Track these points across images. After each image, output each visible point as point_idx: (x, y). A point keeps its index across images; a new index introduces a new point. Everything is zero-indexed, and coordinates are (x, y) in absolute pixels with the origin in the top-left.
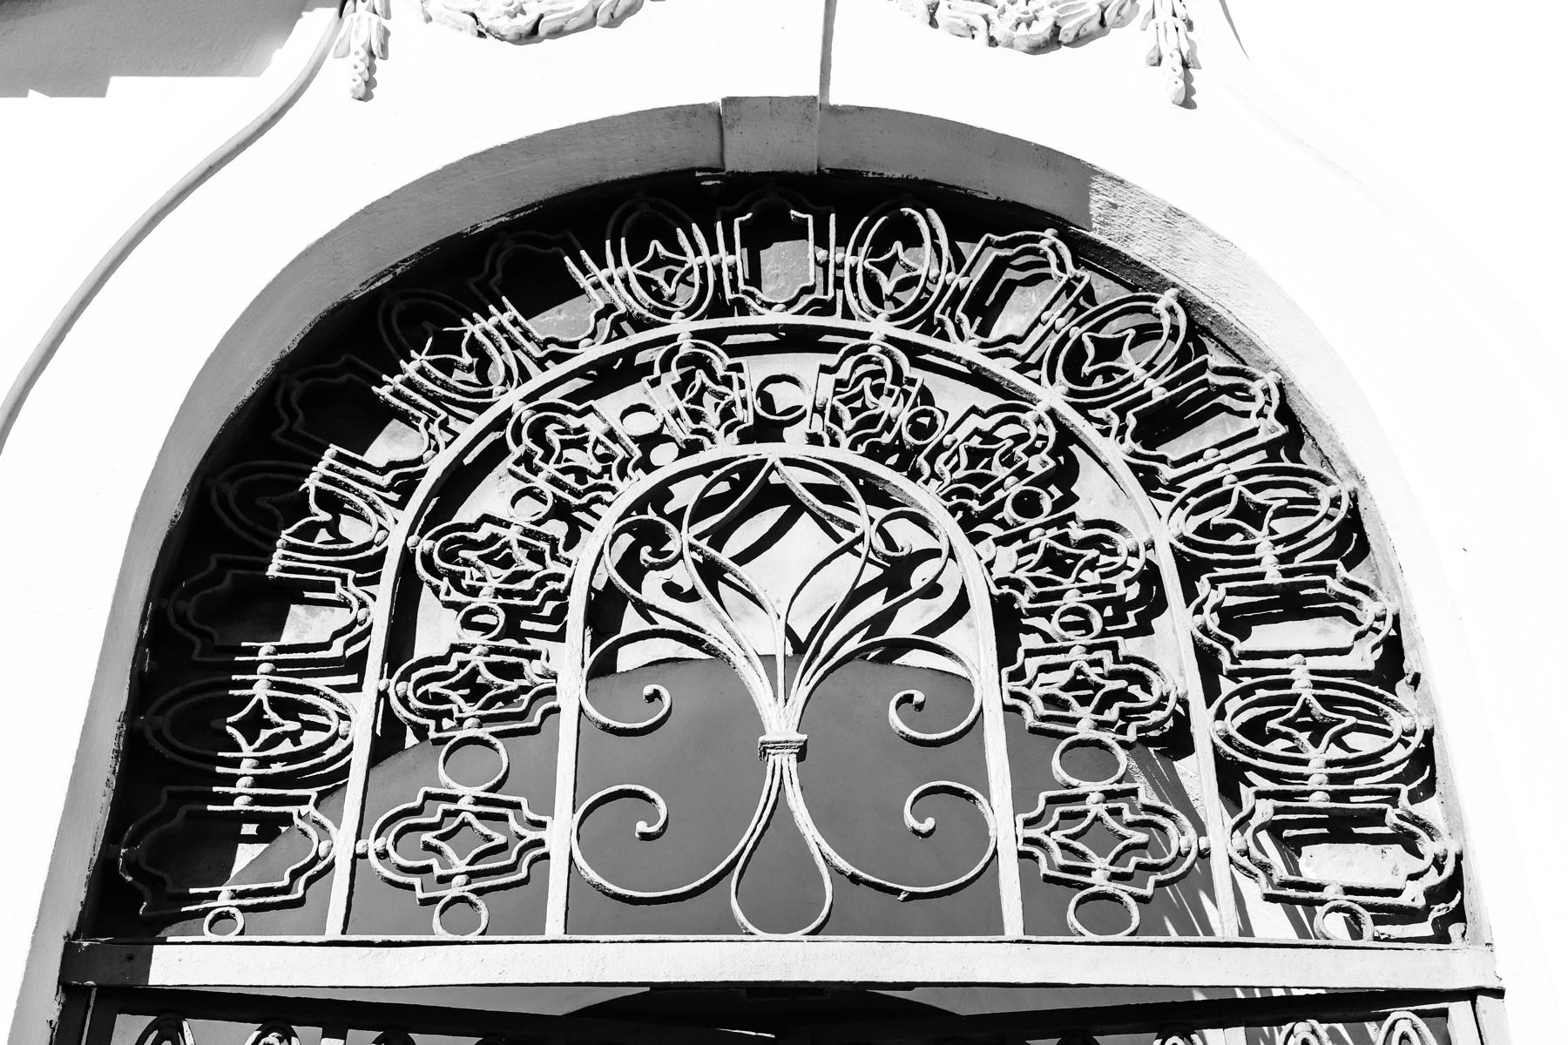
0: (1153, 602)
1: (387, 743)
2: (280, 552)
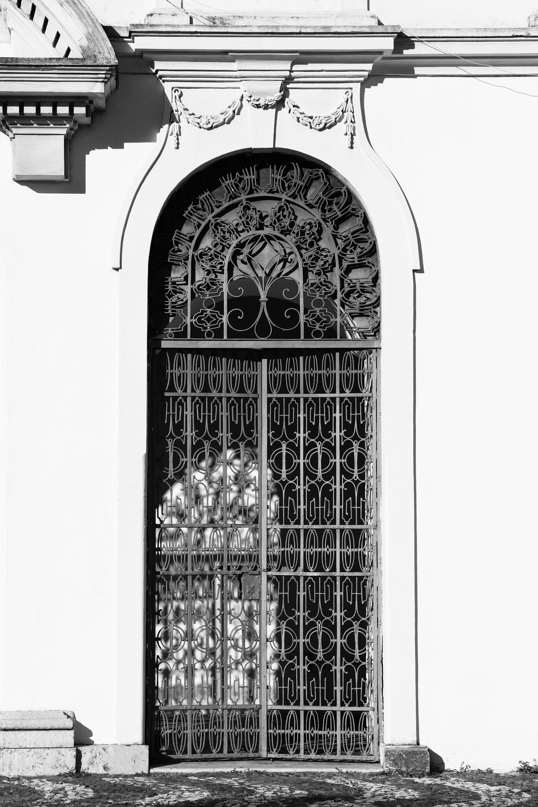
0: (333, 264)
2: (170, 256)
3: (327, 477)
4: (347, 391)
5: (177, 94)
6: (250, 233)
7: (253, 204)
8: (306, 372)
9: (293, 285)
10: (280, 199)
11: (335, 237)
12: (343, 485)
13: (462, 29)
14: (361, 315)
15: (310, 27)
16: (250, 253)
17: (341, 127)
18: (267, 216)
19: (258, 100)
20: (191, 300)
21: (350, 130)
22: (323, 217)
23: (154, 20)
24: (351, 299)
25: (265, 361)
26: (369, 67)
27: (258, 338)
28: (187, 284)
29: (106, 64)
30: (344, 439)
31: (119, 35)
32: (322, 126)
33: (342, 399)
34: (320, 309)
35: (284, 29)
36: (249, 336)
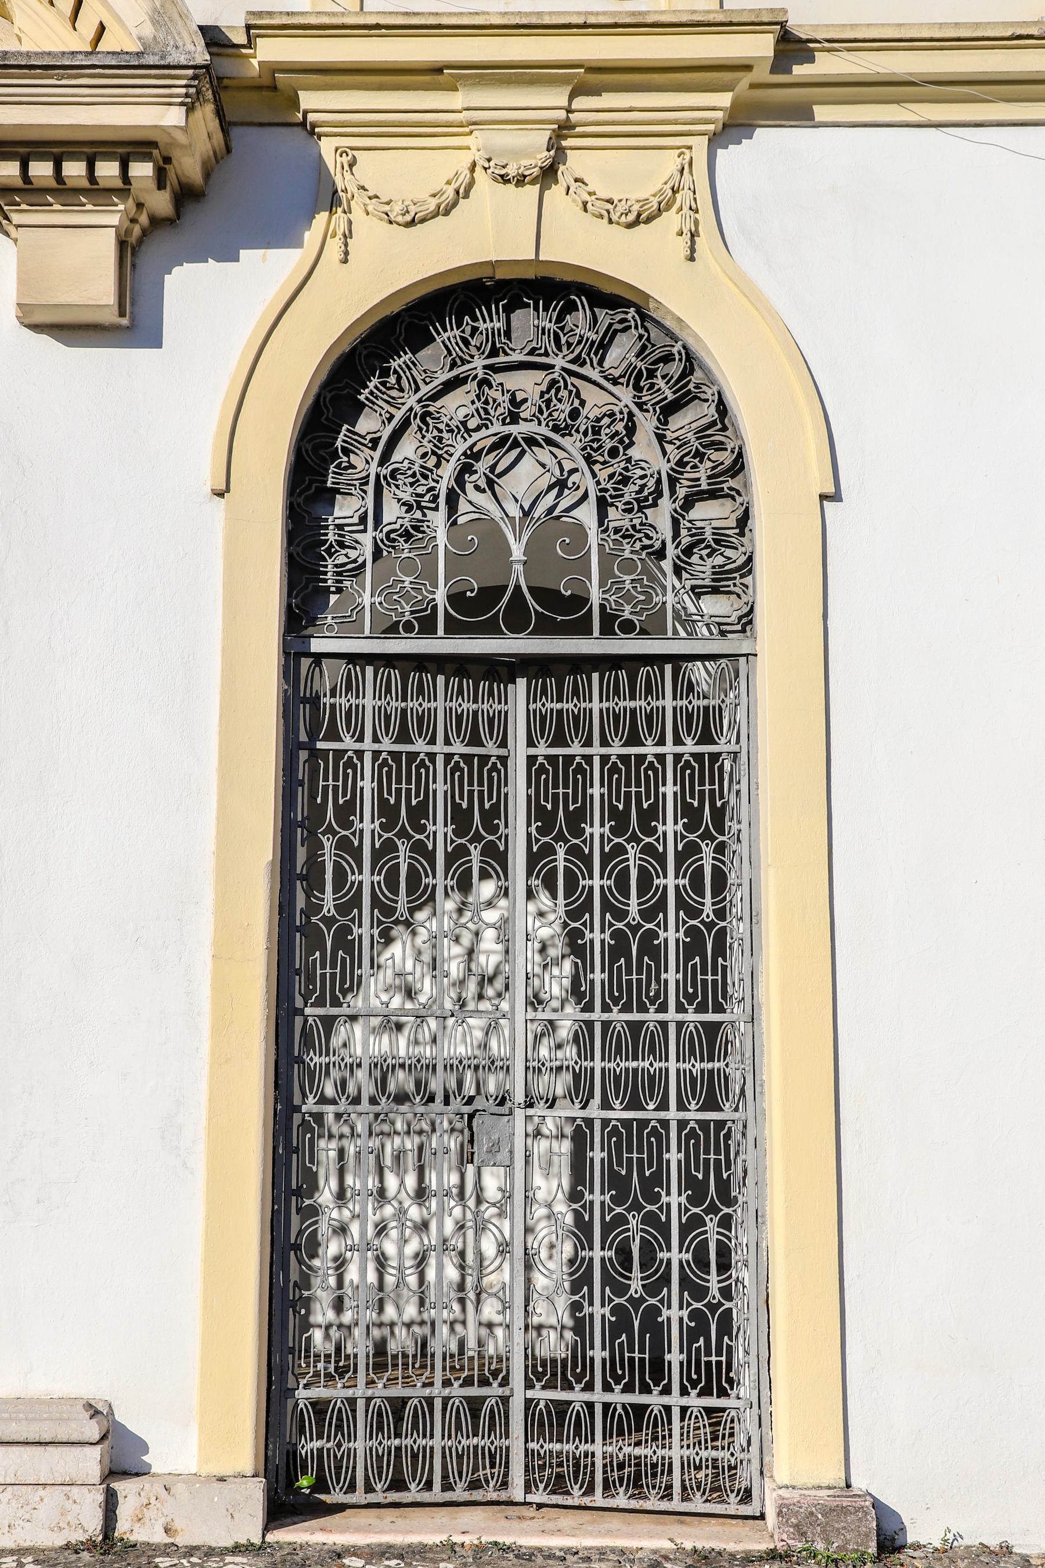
0: (658, 493)
1: (377, 554)
2: (331, 475)
3: (648, 914)
4: (689, 741)
5: (345, 159)
6: (492, 430)
7: (497, 378)
8: (605, 705)
9: (580, 530)
10: (553, 367)
11: (661, 438)
12: (682, 931)
13: (909, 24)
14: (715, 591)
15: (604, 13)
16: (493, 468)
17: (671, 220)
18: (525, 400)
19: (504, 167)
20: (374, 562)
21: (688, 226)
22: (636, 400)
24: (695, 559)
25: (522, 683)
26: (725, 99)
27: (506, 634)
28: (365, 531)
29: (185, 63)
30: (683, 837)
31: (230, 40)
32: (631, 217)
33: (678, 757)
34: (632, 577)
35: (554, 17)
36: (490, 629)
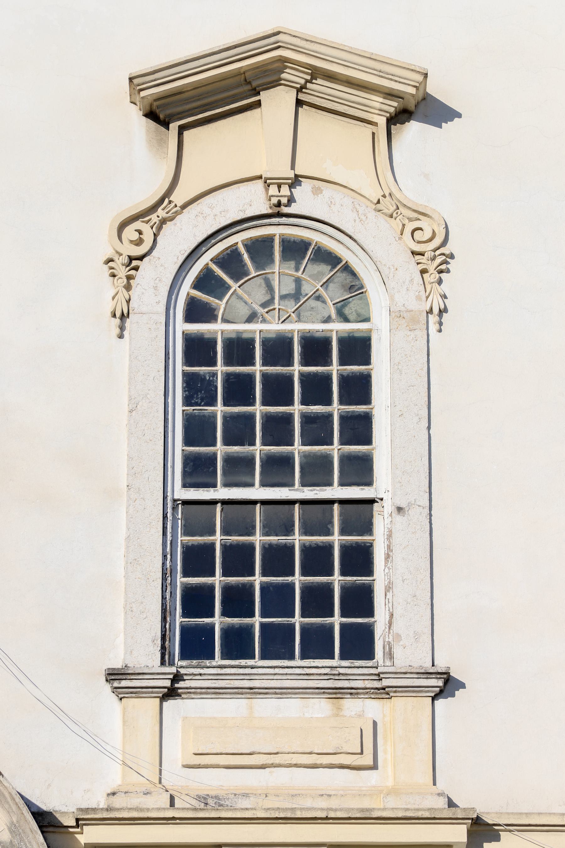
15: (341, 810)
23: (117, 802)
31: (62, 824)
35: (303, 812)
